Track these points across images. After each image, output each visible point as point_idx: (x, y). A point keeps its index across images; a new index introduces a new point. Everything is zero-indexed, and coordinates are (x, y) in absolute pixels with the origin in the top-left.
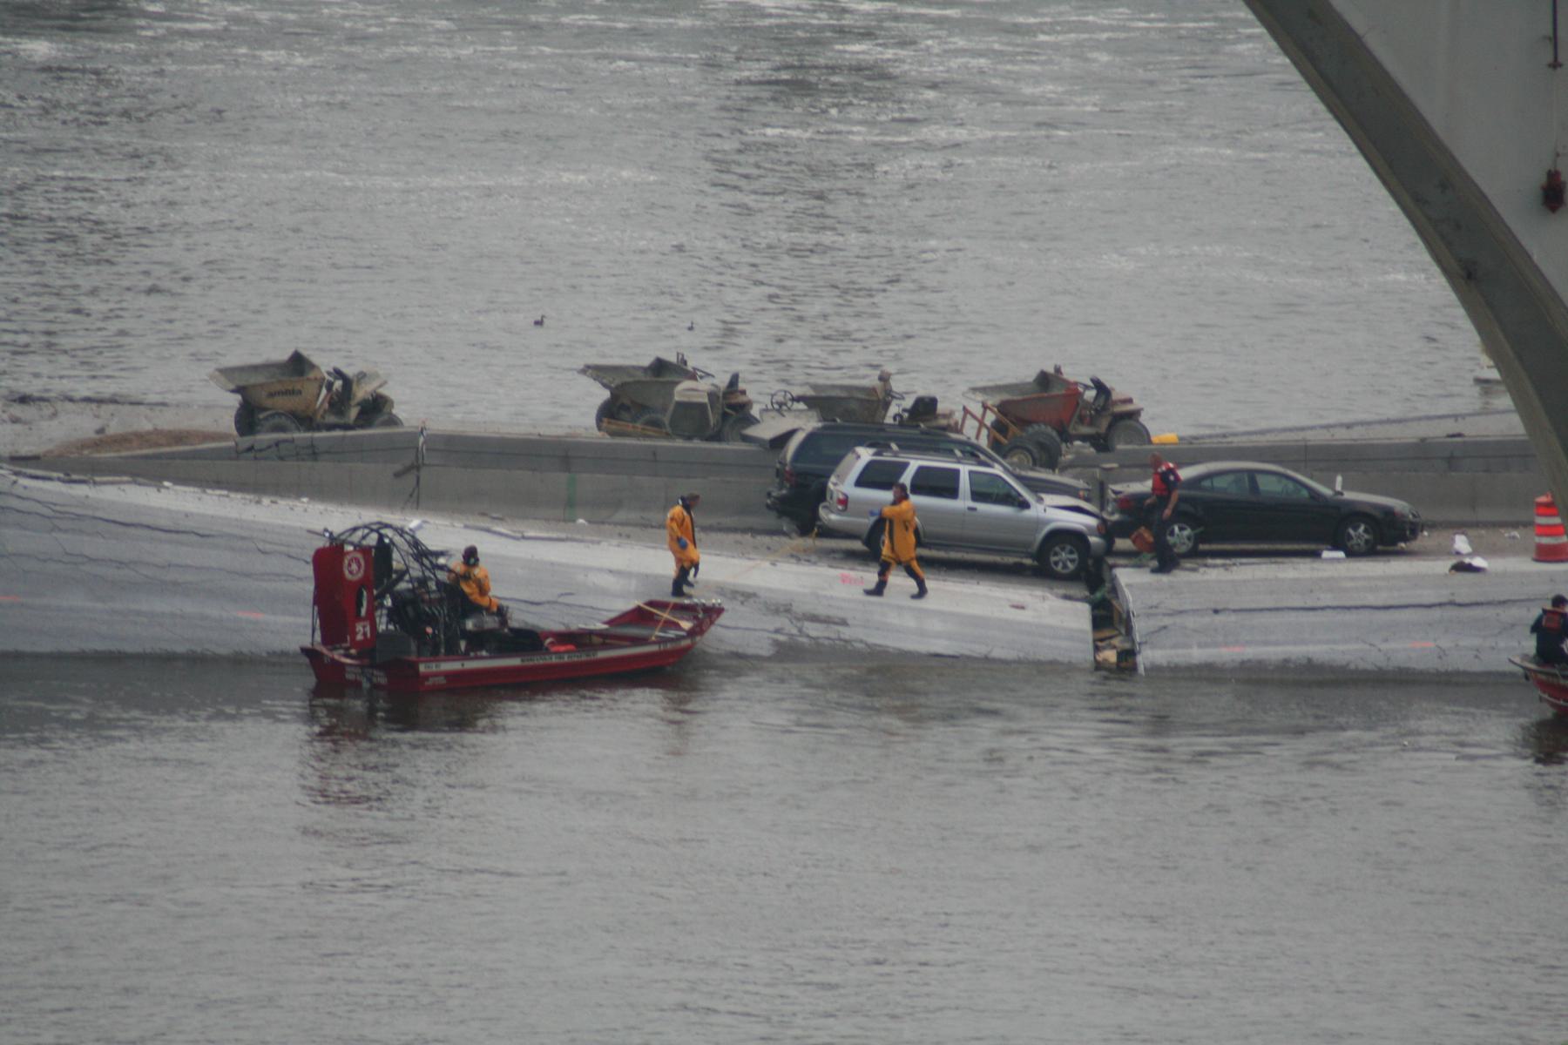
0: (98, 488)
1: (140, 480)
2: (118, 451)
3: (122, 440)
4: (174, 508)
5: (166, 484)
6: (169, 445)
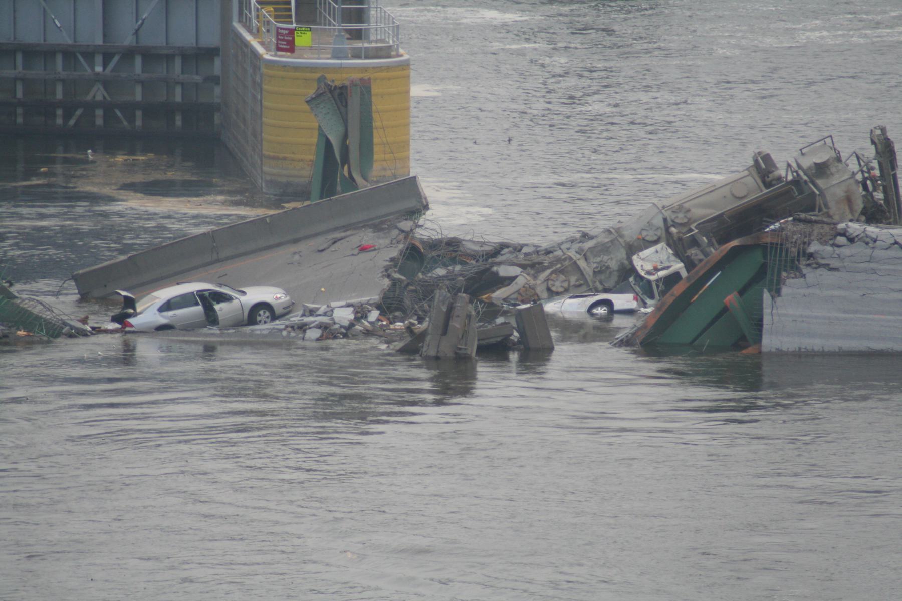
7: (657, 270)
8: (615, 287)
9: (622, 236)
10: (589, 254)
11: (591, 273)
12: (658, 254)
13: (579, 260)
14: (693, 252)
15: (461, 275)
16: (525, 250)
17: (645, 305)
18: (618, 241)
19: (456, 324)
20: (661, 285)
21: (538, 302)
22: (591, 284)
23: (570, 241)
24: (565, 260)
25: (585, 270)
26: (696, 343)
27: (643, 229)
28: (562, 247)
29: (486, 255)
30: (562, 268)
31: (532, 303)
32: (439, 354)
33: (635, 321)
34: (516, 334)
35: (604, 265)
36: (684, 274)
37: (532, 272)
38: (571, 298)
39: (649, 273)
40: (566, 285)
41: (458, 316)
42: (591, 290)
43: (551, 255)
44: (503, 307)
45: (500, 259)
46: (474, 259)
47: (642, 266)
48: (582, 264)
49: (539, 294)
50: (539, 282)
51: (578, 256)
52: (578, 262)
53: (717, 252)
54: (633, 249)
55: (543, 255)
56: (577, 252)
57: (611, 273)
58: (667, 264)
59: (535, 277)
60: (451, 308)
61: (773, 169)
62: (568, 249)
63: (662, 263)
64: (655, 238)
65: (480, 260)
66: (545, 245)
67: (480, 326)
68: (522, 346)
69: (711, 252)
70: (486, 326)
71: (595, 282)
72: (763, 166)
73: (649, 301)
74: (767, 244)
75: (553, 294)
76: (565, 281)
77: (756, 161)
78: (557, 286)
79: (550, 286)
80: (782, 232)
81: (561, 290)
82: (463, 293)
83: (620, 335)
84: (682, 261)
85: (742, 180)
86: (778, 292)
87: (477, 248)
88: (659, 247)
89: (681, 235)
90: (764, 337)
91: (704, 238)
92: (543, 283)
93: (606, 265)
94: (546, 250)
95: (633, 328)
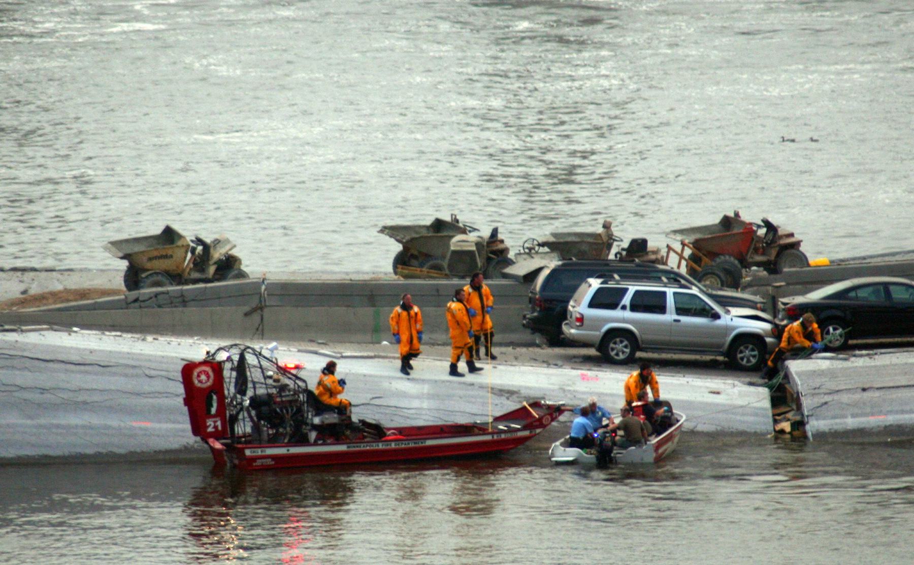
0: (25, 334)
1: (56, 327)
2: (39, 306)
3: (41, 298)
4: (82, 347)
5: (75, 329)
6: (76, 300)
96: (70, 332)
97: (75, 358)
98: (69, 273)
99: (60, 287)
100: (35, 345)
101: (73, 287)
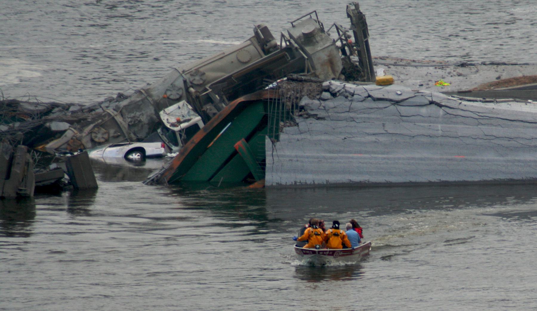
0: (498, 104)
1: (517, 99)
2: (507, 87)
3: (508, 82)
4: (534, 112)
5: (529, 101)
6: (530, 83)
7: (179, 122)
8: (146, 137)
9: (150, 96)
10: (124, 111)
11: (126, 126)
12: (181, 110)
13: (116, 115)
14: (208, 108)
15: (20, 130)
16: (72, 109)
17: (171, 151)
18: (147, 99)
19: (17, 170)
20: (183, 134)
21: (84, 151)
22: (126, 135)
23: (108, 101)
24: (104, 116)
25: (121, 123)
26: (212, 180)
27: (167, 90)
28: (102, 105)
29: (40, 113)
30: (103, 123)
31: (79, 151)
32: (4, 195)
33: (163, 164)
34: (66, 177)
35: (137, 120)
36: (201, 125)
37: (79, 126)
38: (110, 147)
39: (173, 125)
40: (106, 136)
41: (18, 163)
42: (126, 140)
43: (93, 113)
44: (55, 155)
45: (51, 116)
46: (31, 117)
47: (167, 120)
48: (119, 119)
49: (85, 144)
50: (84, 135)
51: (115, 113)
52: (116, 118)
53: (227, 107)
54: (160, 106)
55: (87, 112)
56: (114, 110)
57: (142, 126)
58: (187, 118)
59: (81, 131)
60: (12, 158)
61: (271, 39)
62: (107, 107)
63: (183, 116)
64: (178, 97)
65: (36, 117)
66: (88, 104)
67: (37, 171)
68: (72, 187)
69: (222, 107)
70: (42, 171)
71: (130, 133)
72: (262, 37)
73: (174, 148)
74: (267, 99)
75: (96, 144)
76: (105, 133)
77: (256, 33)
78: (99, 137)
79: (93, 138)
80: (279, 89)
81: (102, 140)
82: (23, 144)
83: (151, 176)
84: (200, 115)
85: (246, 49)
86: (277, 138)
87: (32, 108)
88: (180, 104)
89: (198, 94)
90: (267, 174)
91: (217, 96)
92: (87, 135)
93: (139, 119)
94: (89, 108)
95: (161, 170)
96: (526, 103)
97: (529, 119)
98: (525, 66)
99: (520, 75)
100: (505, 111)
101: (528, 75)
